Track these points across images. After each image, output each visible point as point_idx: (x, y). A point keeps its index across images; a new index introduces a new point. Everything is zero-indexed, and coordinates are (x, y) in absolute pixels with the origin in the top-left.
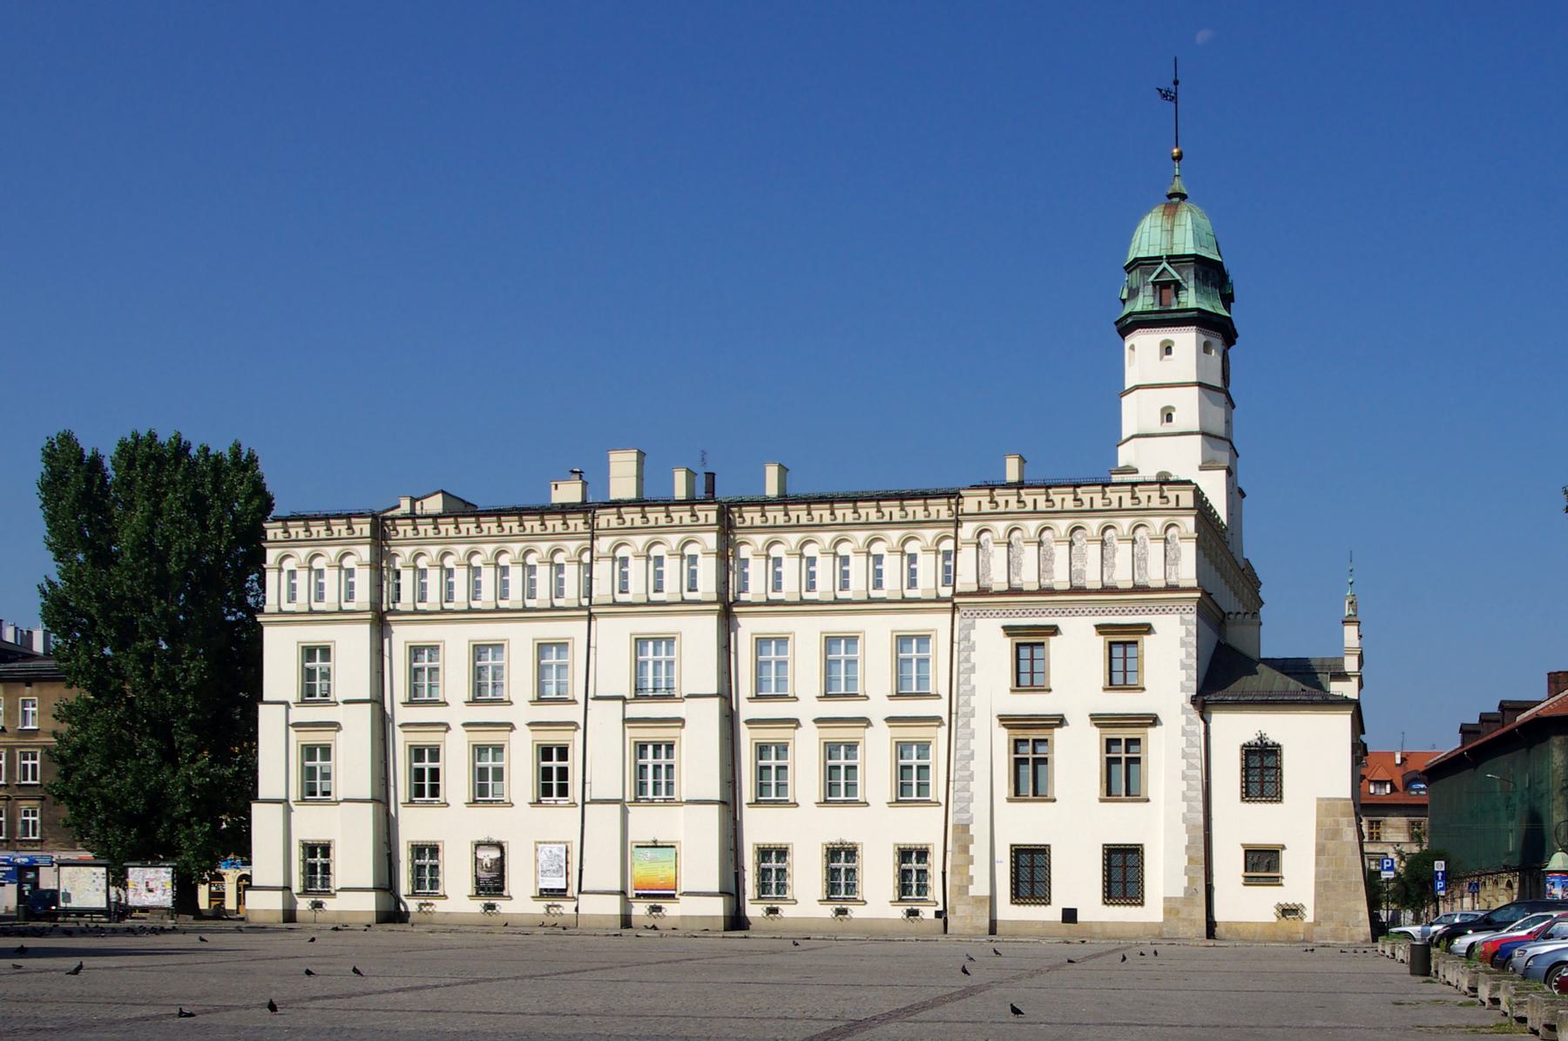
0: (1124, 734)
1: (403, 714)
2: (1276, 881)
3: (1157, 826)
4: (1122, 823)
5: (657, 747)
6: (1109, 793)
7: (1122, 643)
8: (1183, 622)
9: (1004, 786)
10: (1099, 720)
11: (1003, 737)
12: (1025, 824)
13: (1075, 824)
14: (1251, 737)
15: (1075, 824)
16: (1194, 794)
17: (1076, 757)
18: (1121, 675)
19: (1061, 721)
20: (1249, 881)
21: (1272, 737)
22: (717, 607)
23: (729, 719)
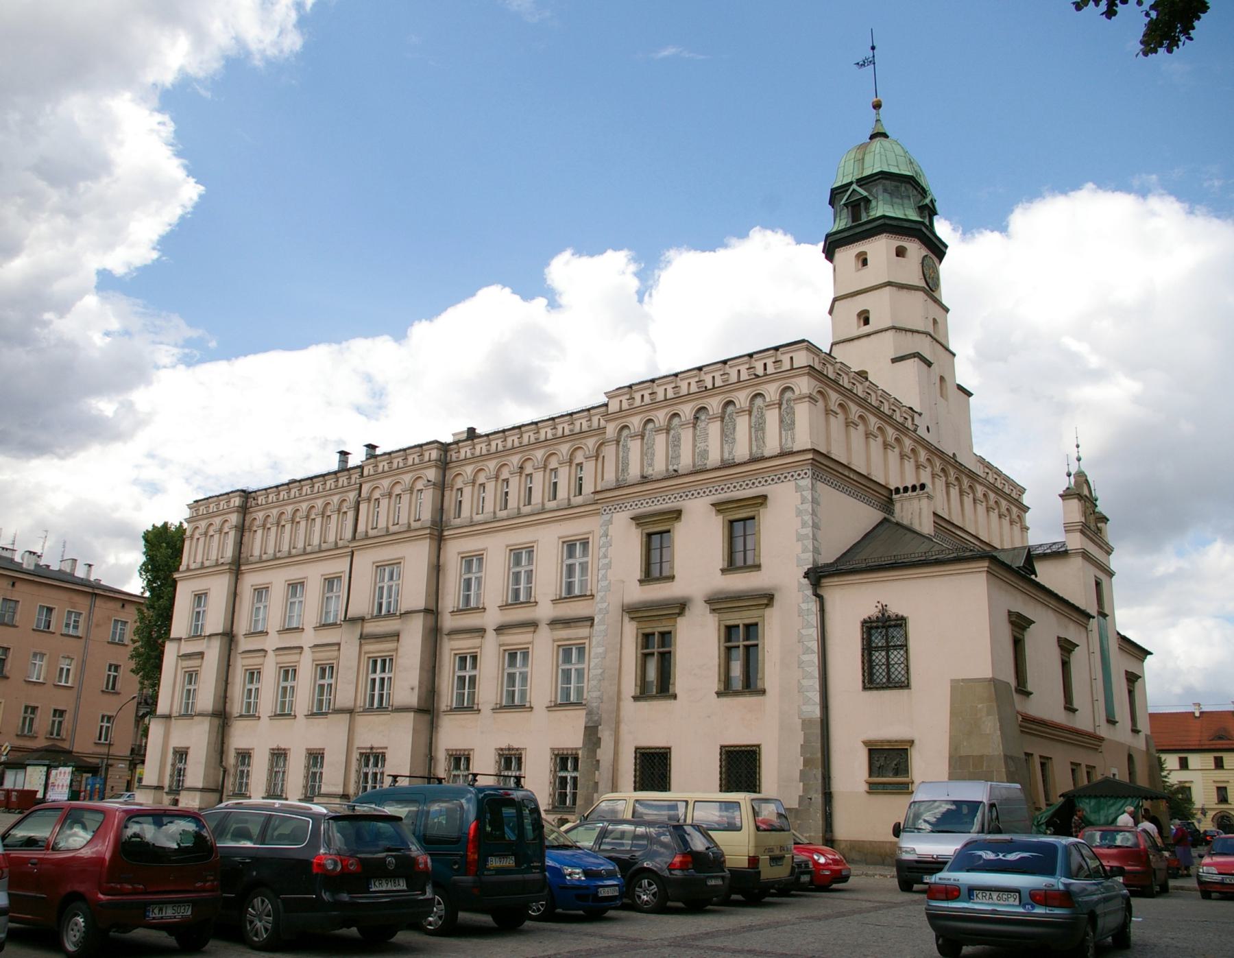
0: (739, 619)
1: (244, 644)
2: (904, 789)
3: (769, 725)
4: (741, 723)
5: (384, 661)
6: (726, 689)
7: (740, 521)
8: (798, 488)
9: (630, 685)
10: (717, 602)
11: (631, 631)
12: (646, 725)
13: (696, 726)
14: (872, 611)
15: (696, 726)
16: (811, 682)
17: (697, 645)
18: (739, 552)
19: (680, 607)
20: (873, 788)
21: (895, 609)
22: (428, 531)
23: (434, 635)
